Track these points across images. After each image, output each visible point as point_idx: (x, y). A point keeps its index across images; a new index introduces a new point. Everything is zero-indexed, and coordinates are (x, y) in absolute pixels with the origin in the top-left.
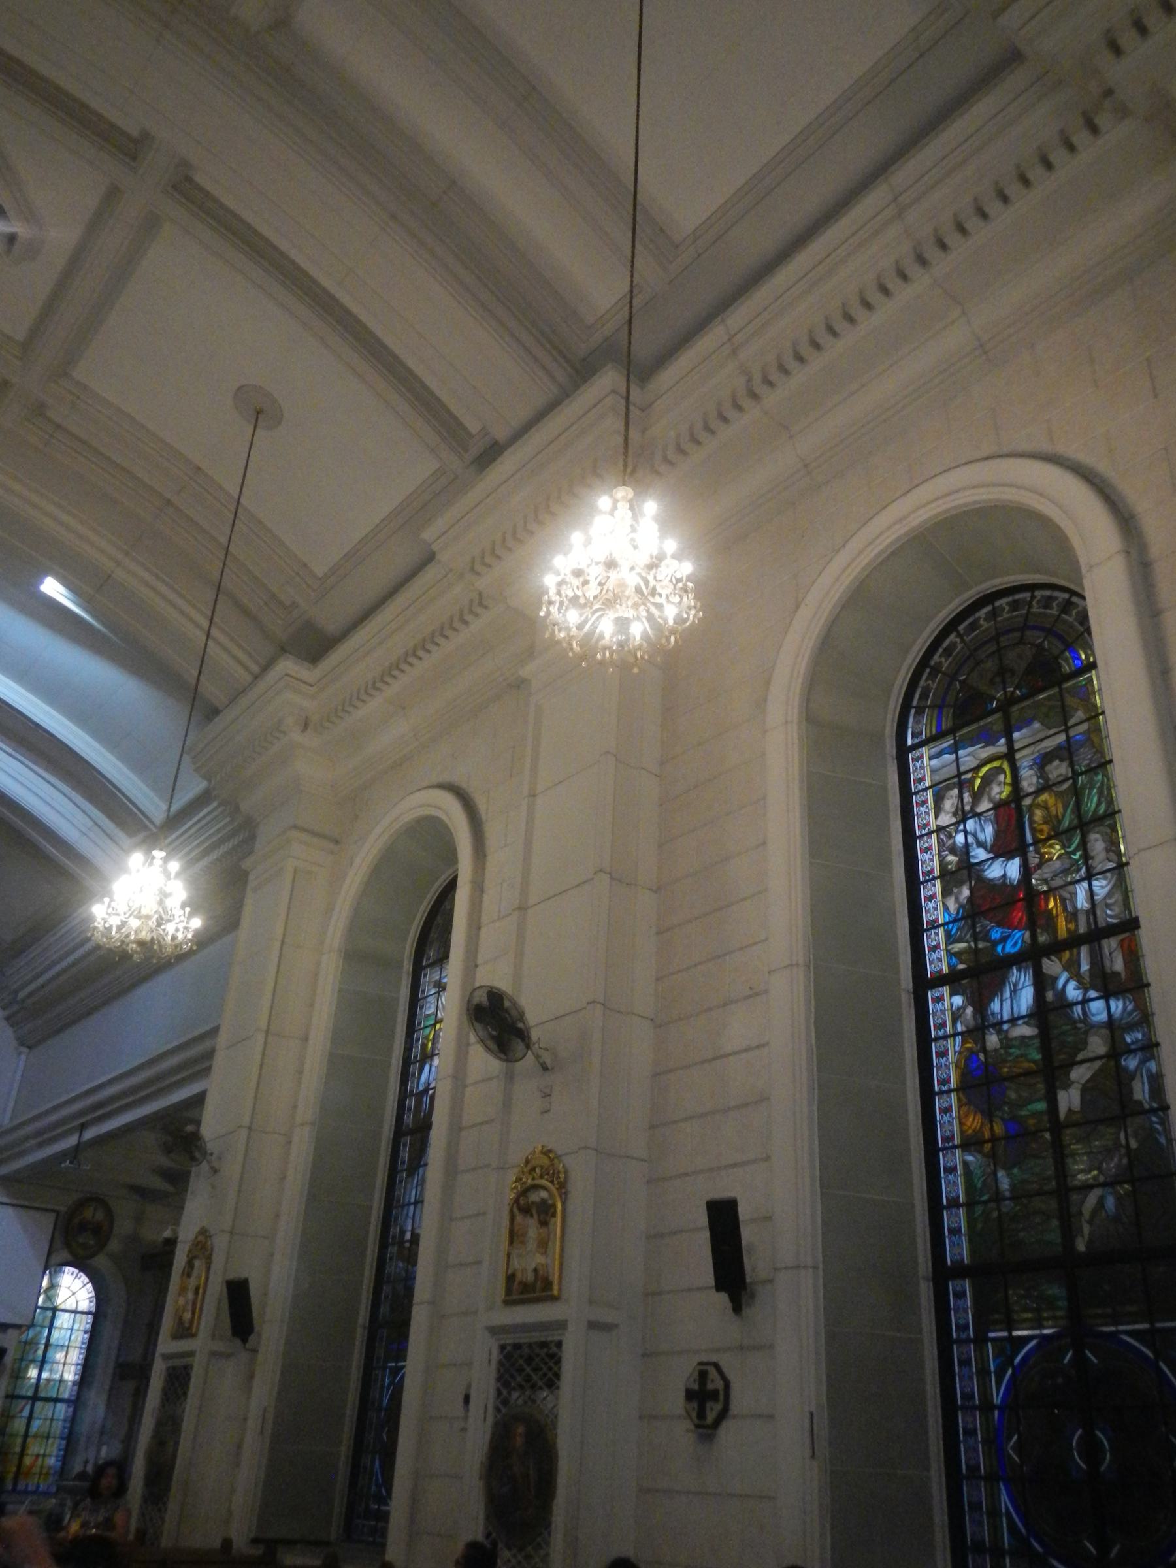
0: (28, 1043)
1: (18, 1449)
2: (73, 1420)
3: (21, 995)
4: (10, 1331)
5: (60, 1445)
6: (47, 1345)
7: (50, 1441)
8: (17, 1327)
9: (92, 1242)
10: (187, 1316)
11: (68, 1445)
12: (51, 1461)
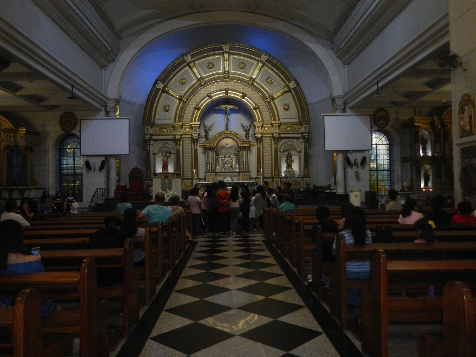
0: (347, 63)
1: (376, 185)
2: (391, 176)
3: (341, 47)
4: (365, 152)
5: (388, 182)
6: (377, 155)
7: (385, 182)
8: (367, 150)
9: (384, 123)
10: (468, 128)
11: (391, 182)
12: (387, 187)
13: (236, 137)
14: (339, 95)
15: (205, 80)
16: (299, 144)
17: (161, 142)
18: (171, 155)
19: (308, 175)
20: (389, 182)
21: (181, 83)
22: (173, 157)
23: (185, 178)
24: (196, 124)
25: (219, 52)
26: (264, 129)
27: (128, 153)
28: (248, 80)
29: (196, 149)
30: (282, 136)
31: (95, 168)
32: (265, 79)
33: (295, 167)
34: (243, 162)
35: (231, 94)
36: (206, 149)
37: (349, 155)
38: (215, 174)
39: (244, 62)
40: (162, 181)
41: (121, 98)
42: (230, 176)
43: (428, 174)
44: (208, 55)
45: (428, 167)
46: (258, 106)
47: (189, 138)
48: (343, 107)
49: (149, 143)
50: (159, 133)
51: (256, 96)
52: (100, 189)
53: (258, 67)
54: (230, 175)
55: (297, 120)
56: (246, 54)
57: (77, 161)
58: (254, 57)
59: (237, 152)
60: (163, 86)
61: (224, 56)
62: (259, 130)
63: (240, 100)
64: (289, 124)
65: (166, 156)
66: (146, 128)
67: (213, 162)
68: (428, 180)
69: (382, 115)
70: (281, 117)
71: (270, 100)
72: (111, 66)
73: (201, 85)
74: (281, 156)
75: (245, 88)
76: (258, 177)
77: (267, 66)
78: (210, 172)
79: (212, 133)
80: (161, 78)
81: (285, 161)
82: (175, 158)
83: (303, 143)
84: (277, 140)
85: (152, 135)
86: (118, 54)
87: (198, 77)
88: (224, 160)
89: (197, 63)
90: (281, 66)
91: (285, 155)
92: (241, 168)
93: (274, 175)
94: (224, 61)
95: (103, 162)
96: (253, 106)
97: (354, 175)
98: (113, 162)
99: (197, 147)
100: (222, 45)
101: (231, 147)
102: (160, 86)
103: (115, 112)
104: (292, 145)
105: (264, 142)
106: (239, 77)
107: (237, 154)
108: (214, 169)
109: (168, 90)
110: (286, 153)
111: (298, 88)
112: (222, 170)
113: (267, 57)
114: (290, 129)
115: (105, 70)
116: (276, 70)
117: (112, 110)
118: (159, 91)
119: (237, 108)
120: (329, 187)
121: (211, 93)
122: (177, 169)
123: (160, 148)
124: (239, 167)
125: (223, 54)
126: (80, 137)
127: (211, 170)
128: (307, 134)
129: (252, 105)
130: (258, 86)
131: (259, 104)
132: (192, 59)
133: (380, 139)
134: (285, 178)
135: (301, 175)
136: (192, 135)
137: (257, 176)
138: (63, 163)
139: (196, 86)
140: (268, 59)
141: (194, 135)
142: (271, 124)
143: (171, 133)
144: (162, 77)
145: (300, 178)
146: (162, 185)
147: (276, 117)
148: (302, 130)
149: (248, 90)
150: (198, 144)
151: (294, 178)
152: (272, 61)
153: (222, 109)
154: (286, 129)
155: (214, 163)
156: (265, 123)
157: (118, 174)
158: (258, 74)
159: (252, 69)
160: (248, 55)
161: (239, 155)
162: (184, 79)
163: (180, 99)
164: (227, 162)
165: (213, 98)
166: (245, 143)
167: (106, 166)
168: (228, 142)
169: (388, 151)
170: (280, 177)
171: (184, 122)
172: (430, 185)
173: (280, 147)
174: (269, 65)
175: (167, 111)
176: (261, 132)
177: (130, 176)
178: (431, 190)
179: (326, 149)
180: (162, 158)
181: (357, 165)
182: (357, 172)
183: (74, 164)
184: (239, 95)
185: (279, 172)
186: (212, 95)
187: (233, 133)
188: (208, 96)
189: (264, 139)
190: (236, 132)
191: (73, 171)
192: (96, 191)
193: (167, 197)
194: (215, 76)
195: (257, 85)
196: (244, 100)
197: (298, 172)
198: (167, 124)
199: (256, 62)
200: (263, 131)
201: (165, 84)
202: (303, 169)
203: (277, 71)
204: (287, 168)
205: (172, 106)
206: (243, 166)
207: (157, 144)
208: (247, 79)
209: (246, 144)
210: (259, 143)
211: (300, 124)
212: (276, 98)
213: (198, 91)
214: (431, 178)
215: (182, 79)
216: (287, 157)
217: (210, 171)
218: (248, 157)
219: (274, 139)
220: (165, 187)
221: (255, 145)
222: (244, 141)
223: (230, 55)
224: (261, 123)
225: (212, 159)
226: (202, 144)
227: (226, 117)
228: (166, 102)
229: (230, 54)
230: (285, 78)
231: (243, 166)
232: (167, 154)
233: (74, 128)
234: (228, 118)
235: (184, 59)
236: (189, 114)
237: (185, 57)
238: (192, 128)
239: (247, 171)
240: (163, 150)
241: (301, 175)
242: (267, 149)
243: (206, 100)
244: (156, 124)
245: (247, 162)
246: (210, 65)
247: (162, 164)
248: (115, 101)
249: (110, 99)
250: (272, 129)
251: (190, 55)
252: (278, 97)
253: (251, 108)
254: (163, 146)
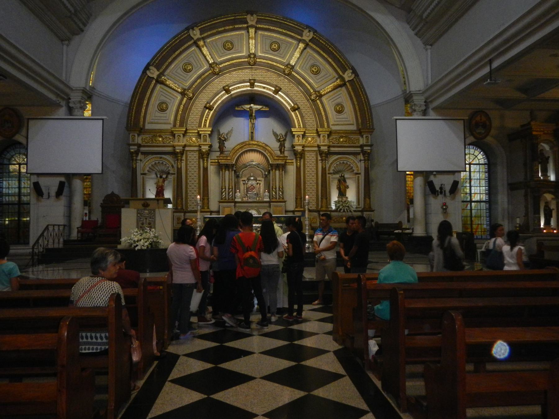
0: (429, 43)
1: (469, 222)
3: (424, 16)
4: (456, 174)
12: (485, 226)
13: (265, 149)
14: (417, 89)
15: (221, 66)
16: (356, 162)
17: (155, 156)
18: (169, 177)
19: (370, 207)
20: (488, 218)
21: (185, 70)
22: (172, 180)
23: (189, 210)
24: (206, 130)
25: (241, 26)
26: (307, 140)
27: (100, 172)
28: (283, 67)
29: (205, 167)
30: (332, 149)
31: (49, 193)
32: (308, 67)
33: (351, 195)
34: (276, 186)
35: (259, 88)
36: (221, 167)
37: (432, 178)
38: (233, 204)
39: (277, 41)
40: (138, 213)
41: (96, 91)
42: (256, 208)
43: (549, 208)
44: (225, 29)
45: (548, 197)
46: (298, 105)
47: (196, 151)
48: (424, 108)
49: (135, 157)
50: (151, 143)
51: (295, 90)
52: (54, 225)
53: (298, 50)
54: (256, 206)
55: (354, 128)
56: (281, 30)
57: (24, 182)
58: (292, 34)
59: (266, 173)
60: (157, 73)
61: (248, 32)
62: (299, 141)
63: (272, 97)
64: (343, 133)
65: (161, 177)
66: (131, 134)
67: (231, 187)
68: (551, 216)
69: (481, 120)
70: (331, 122)
71: (316, 97)
72: (77, 38)
73: (214, 74)
74: (331, 179)
75: (280, 78)
76: (296, 209)
77: (311, 48)
78: (226, 201)
79: (229, 145)
80: (155, 62)
81: (336, 187)
82: (174, 180)
83: (363, 161)
84: (324, 155)
85: (139, 146)
86: (88, 22)
87: (210, 62)
88: (247, 184)
89: (208, 40)
90: (332, 48)
91: (337, 178)
92: (272, 195)
93: (320, 207)
94: (249, 40)
95: (62, 185)
96: (291, 106)
97: (440, 207)
98: (77, 184)
99: (207, 164)
100: (246, 15)
101: (258, 165)
102: (153, 74)
103: (83, 108)
104: (347, 163)
105: (306, 158)
106: (270, 62)
107: (266, 176)
108: (232, 196)
109: (165, 79)
110: (338, 176)
111: (356, 80)
112: (244, 199)
113: (311, 35)
114: (345, 140)
115: (68, 45)
116: (324, 55)
117: (78, 105)
118: (152, 81)
119: (267, 109)
120: (399, 226)
121: (229, 85)
122: (177, 197)
123: (152, 165)
124: (270, 195)
125: (247, 29)
126: (26, 147)
127: (227, 199)
128: (369, 148)
129: (289, 104)
130: (298, 77)
131: (299, 103)
132: (201, 34)
133: (475, 157)
134: (336, 211)
135: (359, 208)
136: (200, 146)
137: (296, 208)
138: (2, 185)
139: (206, 74)
140: (313, 37)
141: (203, 147)
142: (317, 132)
143: (169, 142)
144: (156, 60)
145: (359, 211)
146: (137, 220)
147: (324, 123)
148: (362, 141)
149: (284, 83)
150: (209, 159)
151: (350, 211)
152: (319, 41)
153: (245, 111)
154: (339, 140)
155: (232, 189)
156: (309, 130)
157: (86, 203)
158: (299, 58)
159: (290, 52)
160: (283, 31)
161: (270, 176)
162: (189, 65)
163: (183, 94)
164: (252, 187)
165: (232, 93)
166: (278, 160)
167: (66, 190)
168: (254, 158)
169: (487, 174)
170: (330, 209)
171: (189, 127)
172: (553, 223)
173: (330, 167)
174: (315, 47)
175: (162, 110)
176: (302, 144)
177: (102, 206)
178: (555, 231)
179: (399, 170)
180: (156, 181)
181: (443, 193)
182: (445, 203)
183: (20, 188)
184: (270, 90)
185: (328, 203)
186: (230, 88)
187: (261, 144)
188: (225, 90)
189: (307, 155)
190: (266, 143)
191: (17, 198)
192: (47, 228)
193: (145, 240)
194: (235, 61)
195: (296, 75)
196: (277, 96)
197: (355, 203)
198: (162, 130)
199: (295, 42)
200: (305, 142)
201: (161, 70)
202: (363, 199)
203: (326, 56)
204: (338, 197)
205: (171, 104)
206: (276, 193)
207: (148, 159)
208: (281, 66)
209: (280, 161)
210: (298, 159)
211: (360, 132)
212: (324, 95)
213: (210, 83)
214: (554, 214)
215: (186, 64)
216: (339, 181)
217: (226, 199)
218: (282, 180)
219: (321, 154)
220: (143, 224)
221: (293, 162)
222: (277, 157)
223: (257, 31)
224: (302, 130)
225: (229, 182)
226: (214, 160)
227: (251, 121)
228: (163, 98)
229: (257, 29)
230: (338, 66)
231: (276, 193)
232: (163, 175)
233: (18, 132)
234: (253, 124)
235: (190, 34)
236: (196, 116)
237: (191, 31)
238: (199, 135)
239: (281, 200)
240: (157, 168)
241: (361, 208)
242: (311, 169)
243: (222, 96)
244: (147, 130)
245: (281, 187)
246: (228, 45)
247: (156, 189)
248: (82, 92)
249: (74, 89)
250: (318, 139)
251: (199, 29)
252: (327, 93)
253: (287, 108)
254: (157, 162)
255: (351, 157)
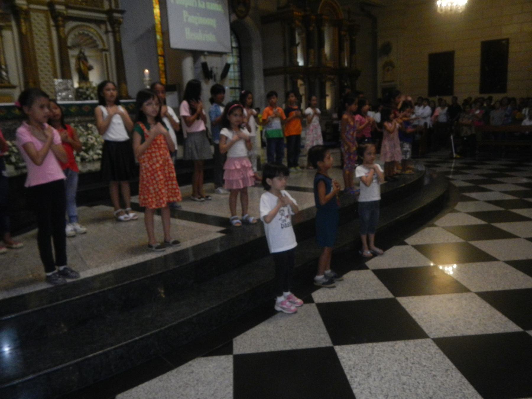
4: (224, 56)
181: (213, 78)
255: (92, 26)
